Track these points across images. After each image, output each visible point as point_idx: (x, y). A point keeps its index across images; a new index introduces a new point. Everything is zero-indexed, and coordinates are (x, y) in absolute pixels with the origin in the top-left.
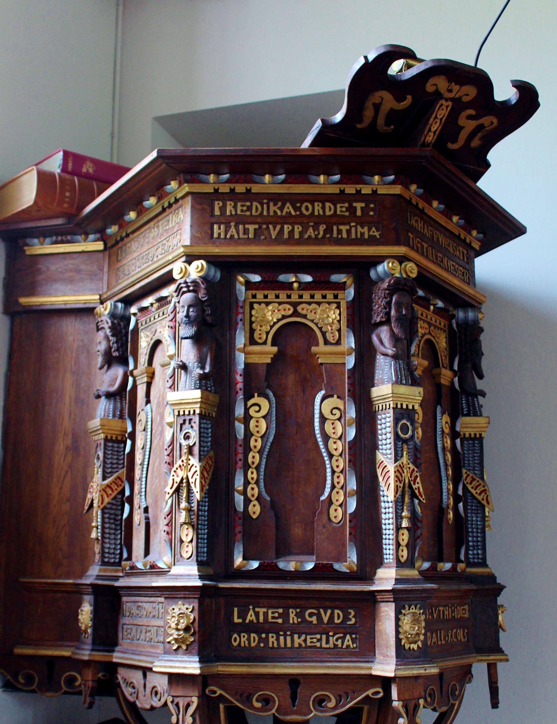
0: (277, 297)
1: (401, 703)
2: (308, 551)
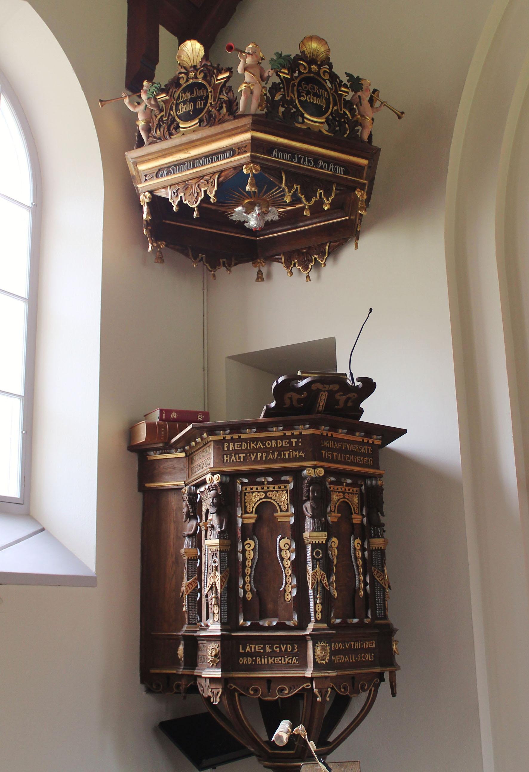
0: (257, 489)
1: (317, 690)
2: (275, 616)
